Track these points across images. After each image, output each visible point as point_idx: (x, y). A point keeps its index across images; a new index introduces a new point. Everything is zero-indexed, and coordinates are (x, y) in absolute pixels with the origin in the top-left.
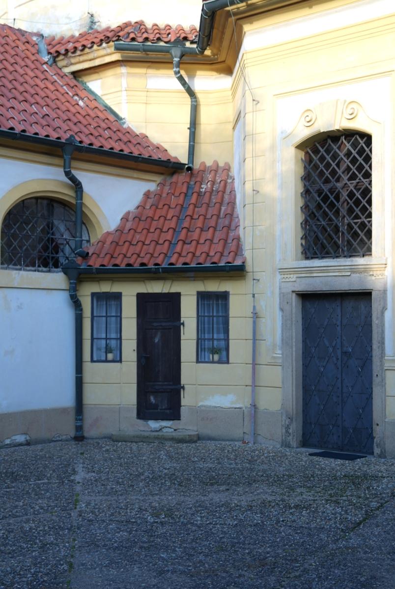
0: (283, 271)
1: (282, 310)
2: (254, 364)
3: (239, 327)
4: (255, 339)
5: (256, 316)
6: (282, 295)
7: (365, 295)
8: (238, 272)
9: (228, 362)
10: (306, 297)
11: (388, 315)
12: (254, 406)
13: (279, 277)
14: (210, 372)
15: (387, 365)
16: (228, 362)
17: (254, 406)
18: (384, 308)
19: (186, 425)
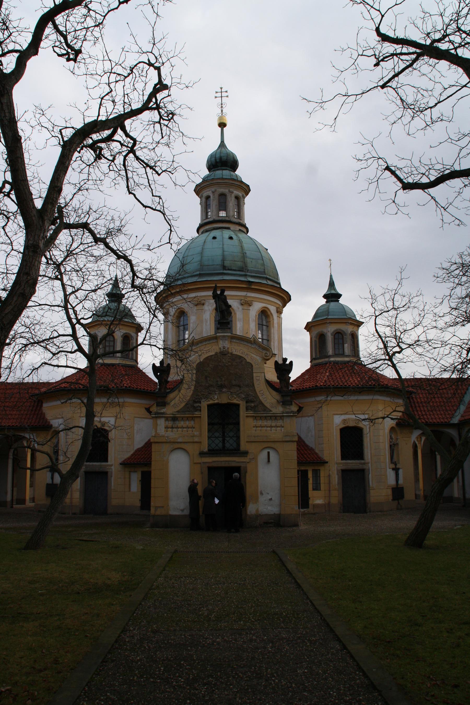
0: (337, 463)
1: (338, 474)
2: (330, 490)
3: (323, 480)
4: (329, 483)
5: (329, 476)
6: (338, 470)
7: (363, 471)
8: (324, 463)
9: (320, 490)
10: (343, 471)
11: (370, 475)
12: (329, 503)
13: (336, 465)
14: (316, 493)
15: (370, 488)
16: (320, 490)
17: (329, 503)
18: (369, 474)
19: (310, 509)
